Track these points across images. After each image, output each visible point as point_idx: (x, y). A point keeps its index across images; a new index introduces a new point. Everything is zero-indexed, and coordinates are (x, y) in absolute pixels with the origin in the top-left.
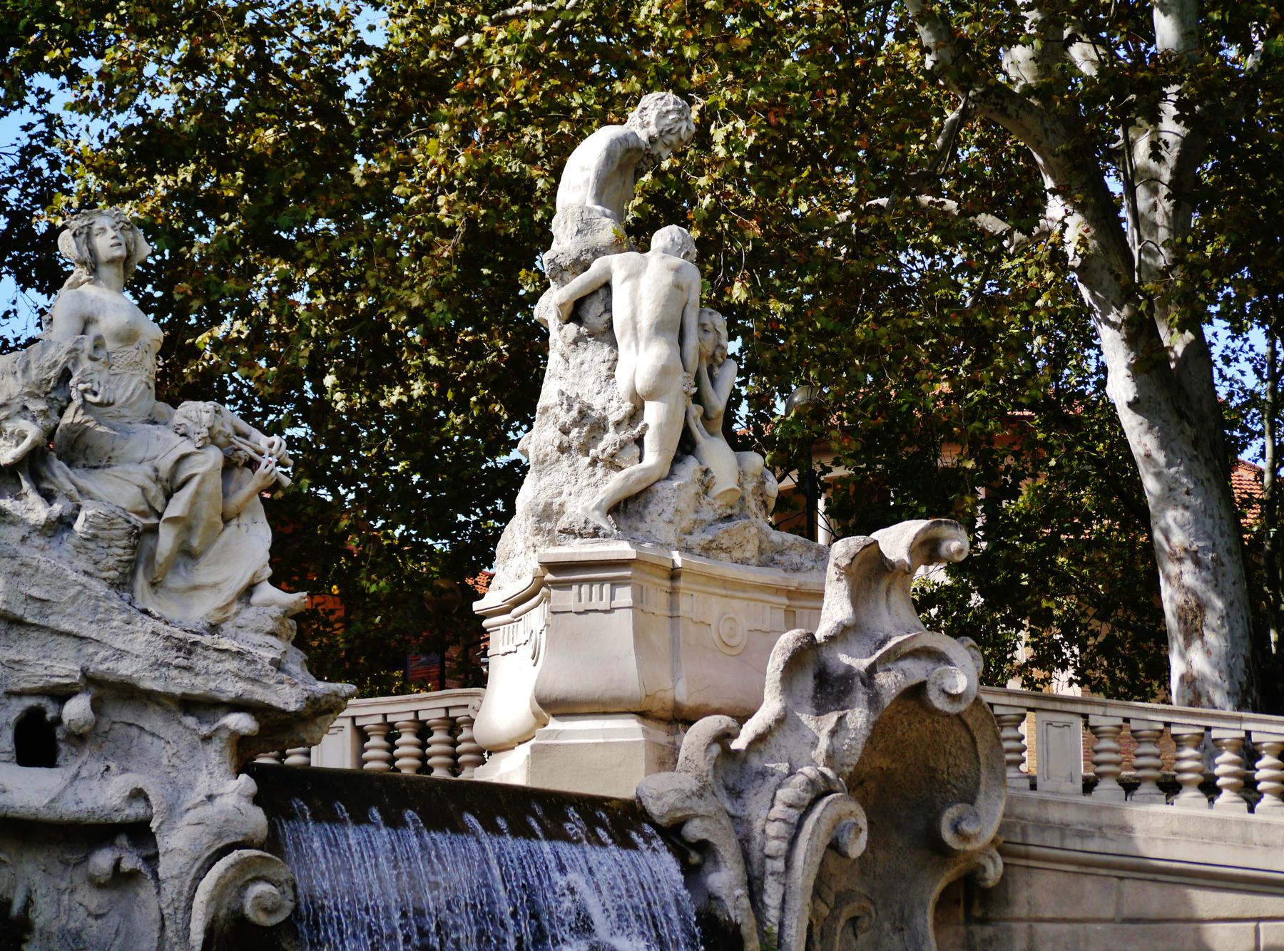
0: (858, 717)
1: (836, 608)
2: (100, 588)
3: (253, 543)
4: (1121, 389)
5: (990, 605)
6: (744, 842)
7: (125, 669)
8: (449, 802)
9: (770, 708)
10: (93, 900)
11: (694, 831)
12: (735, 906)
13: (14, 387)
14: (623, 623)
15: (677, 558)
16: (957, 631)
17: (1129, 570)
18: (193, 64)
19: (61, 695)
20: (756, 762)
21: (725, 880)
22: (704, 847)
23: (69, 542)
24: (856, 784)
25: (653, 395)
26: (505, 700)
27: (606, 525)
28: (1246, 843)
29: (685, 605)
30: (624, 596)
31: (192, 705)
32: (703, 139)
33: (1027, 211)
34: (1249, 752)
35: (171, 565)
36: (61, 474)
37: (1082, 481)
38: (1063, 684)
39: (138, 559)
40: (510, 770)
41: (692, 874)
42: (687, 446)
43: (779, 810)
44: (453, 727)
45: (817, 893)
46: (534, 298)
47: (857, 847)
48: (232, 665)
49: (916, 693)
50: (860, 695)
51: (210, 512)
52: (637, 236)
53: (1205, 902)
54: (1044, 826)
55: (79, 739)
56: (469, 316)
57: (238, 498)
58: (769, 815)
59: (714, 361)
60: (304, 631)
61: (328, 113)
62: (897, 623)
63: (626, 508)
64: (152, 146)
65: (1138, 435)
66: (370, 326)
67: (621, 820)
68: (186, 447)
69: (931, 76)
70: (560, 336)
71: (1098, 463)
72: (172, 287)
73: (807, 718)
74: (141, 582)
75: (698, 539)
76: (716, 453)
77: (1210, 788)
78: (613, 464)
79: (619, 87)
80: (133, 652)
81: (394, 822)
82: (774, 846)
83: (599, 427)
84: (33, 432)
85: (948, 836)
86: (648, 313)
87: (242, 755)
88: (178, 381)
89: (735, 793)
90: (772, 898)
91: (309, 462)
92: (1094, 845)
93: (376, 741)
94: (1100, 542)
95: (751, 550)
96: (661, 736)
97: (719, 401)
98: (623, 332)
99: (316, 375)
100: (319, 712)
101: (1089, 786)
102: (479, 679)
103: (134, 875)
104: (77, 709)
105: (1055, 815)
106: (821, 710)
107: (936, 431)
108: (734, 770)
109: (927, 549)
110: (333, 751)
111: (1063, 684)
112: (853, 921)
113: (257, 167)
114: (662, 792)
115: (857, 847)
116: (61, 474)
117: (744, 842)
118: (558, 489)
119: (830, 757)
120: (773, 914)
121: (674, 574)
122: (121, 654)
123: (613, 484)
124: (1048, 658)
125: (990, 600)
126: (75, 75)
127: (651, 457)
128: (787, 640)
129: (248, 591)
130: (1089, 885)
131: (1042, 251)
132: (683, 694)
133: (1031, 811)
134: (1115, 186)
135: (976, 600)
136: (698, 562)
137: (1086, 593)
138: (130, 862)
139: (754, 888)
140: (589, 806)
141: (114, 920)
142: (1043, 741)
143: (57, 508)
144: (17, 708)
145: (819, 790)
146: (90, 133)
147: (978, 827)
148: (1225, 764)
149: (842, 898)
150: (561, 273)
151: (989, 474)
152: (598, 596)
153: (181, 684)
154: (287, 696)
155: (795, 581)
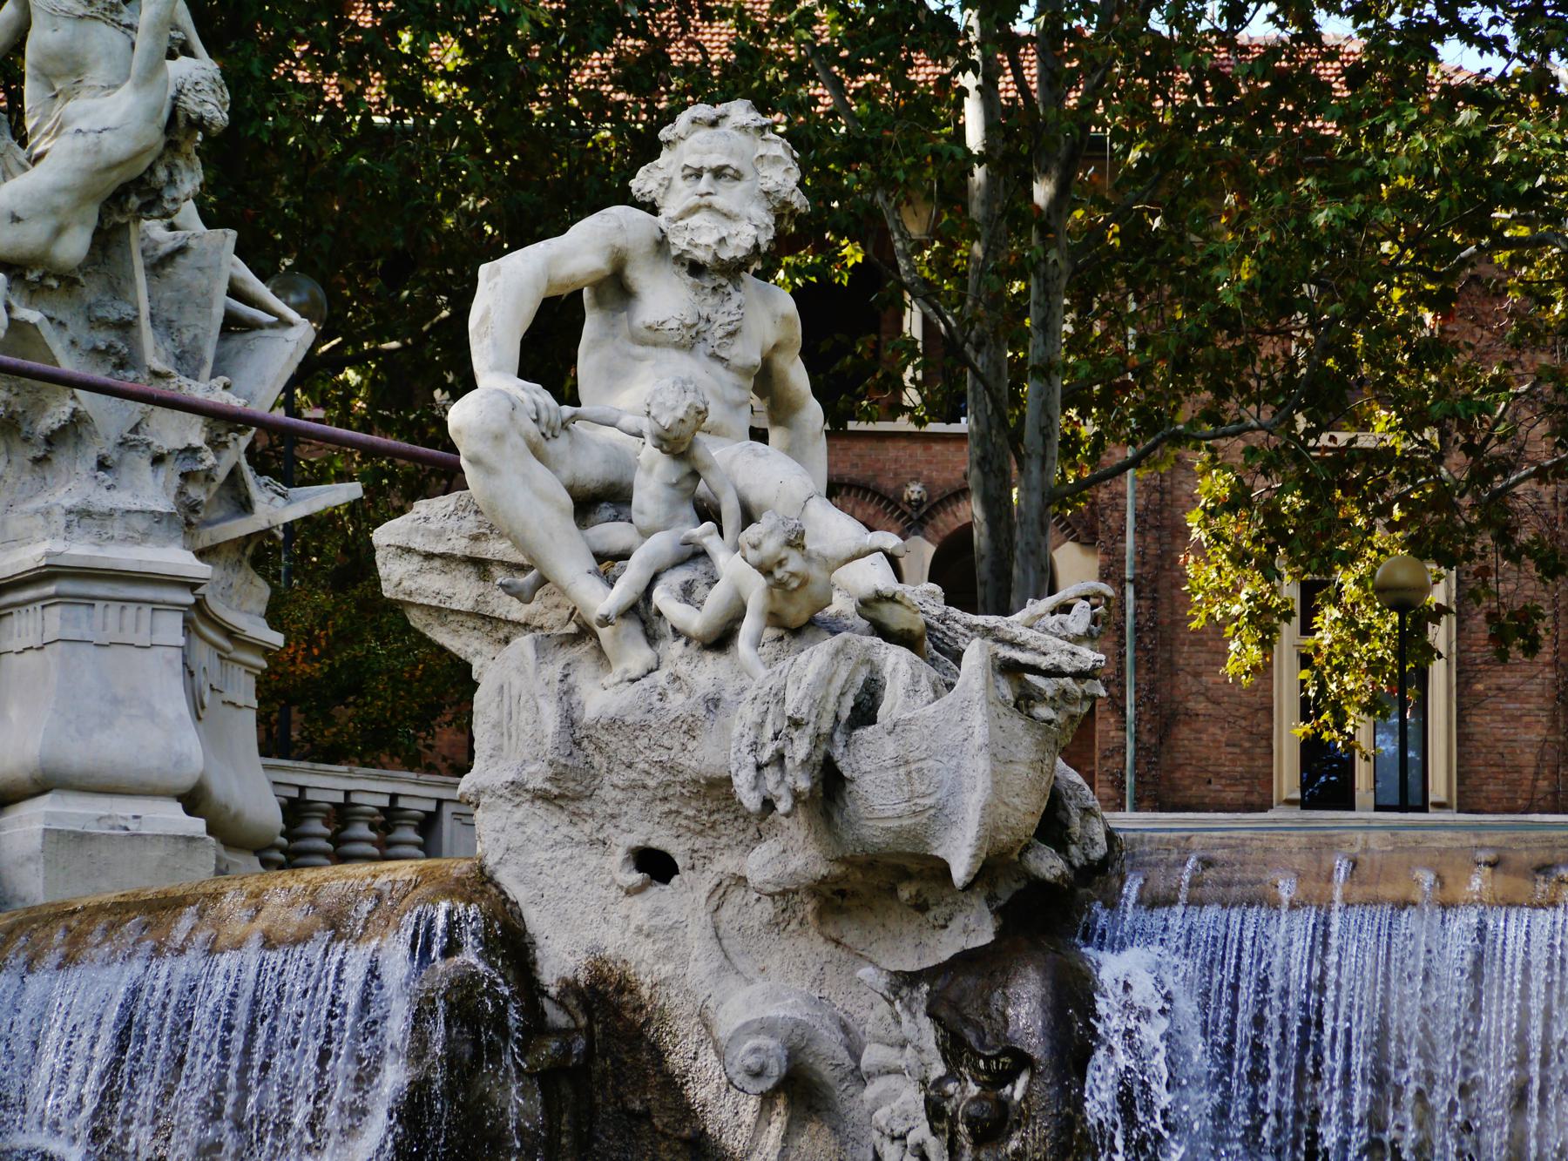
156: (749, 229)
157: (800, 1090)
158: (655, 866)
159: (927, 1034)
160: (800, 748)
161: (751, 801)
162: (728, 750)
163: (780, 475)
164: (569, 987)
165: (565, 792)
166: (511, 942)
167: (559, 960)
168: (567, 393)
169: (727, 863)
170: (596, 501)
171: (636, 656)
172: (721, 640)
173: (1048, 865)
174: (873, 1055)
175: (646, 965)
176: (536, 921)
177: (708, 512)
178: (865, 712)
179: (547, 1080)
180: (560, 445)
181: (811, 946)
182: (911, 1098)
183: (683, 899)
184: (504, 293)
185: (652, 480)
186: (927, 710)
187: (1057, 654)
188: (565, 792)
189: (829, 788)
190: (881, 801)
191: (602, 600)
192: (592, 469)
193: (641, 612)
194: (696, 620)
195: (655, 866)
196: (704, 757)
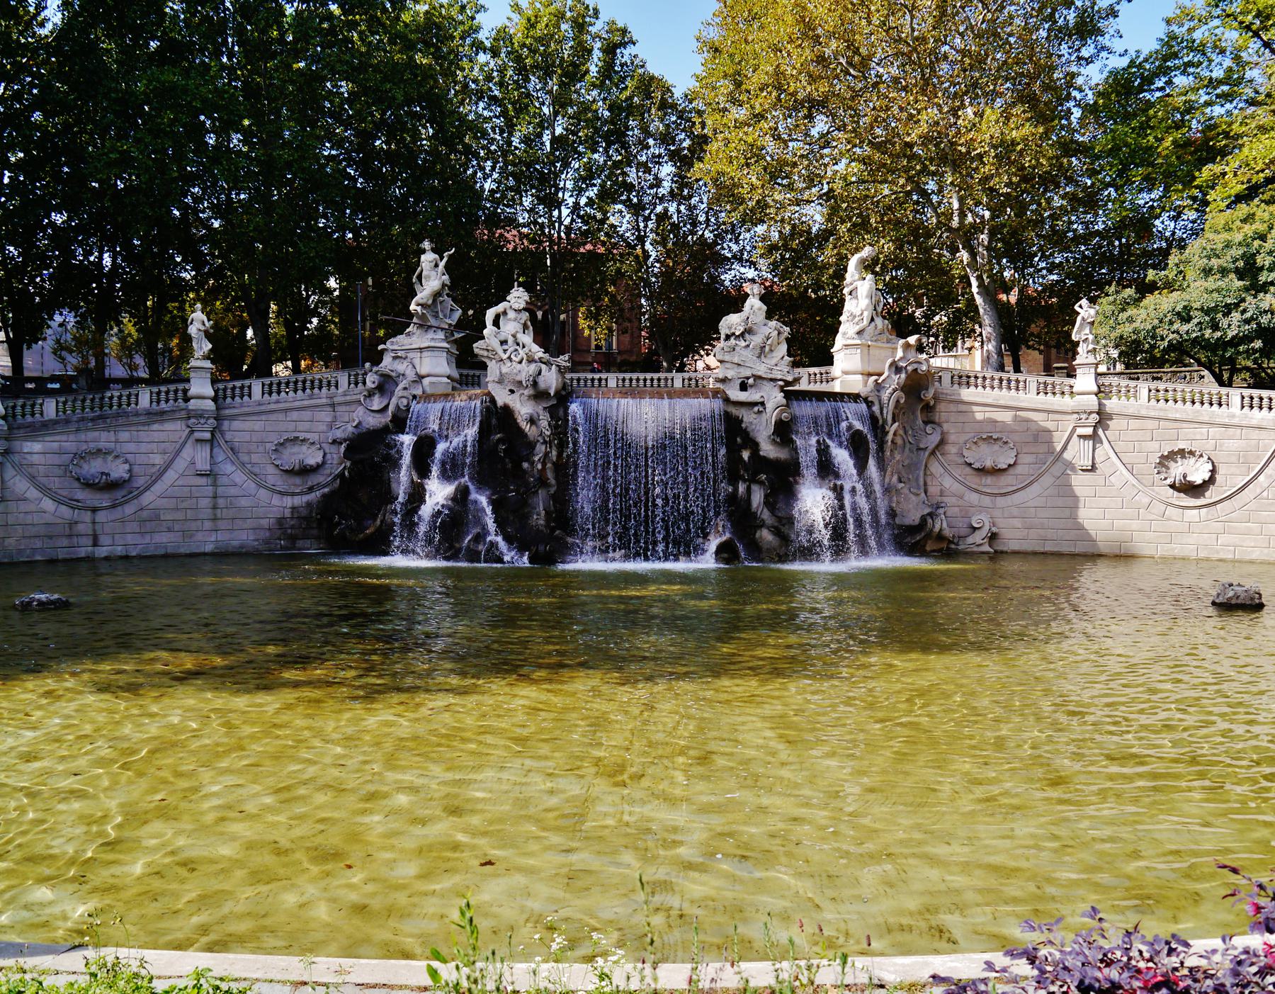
0: (903, 376)
1: (900, 354)
3: (784, 348)
19: (748, 378)
21: (876, 409)
26: (836, 370)
31: (771, 380)
34: (984, 378)
36: (747, 335)
39: (762, 352)
42: (872, 320)
47: (902, 401)
53: (975, 408)
58: (885, 396)
63: (860, 333)
67: (855, 397)
70: (848, 298)
77: (976, 386)
80: (761, 370)
81: (811, 400)
84: (742, 329)
86: (865, 293)
97: (879, 309)
98: (860, 296)
102: (832, 364)
104: (751, 381)
108: (878, 387)
115: (902, 401)
116: (747, 335)
123: (857, 328)
128: (890, 360)
140: (849, 395)
145: (895, 391)
148: (980, 381)
152: (853, 351)
153: (770, 376)
156: (523, 305)
157: (532, 421)
158: (512, 391)
162: (522, 377)
163: (527, 339)
165: (500, 382)
166: (493, 400)
167: (500, 403)
170: (504, 342)
171: (509, 364)
172: (520, 362)
175: (511, 404)
178: (540, 373)
179: (498, 419)
183: (516, 395)
184: (490, 314)
188: (500, 382)
189: (535, 384)
190: (542, 385)
191: (505, 357)
192: (502, 339)
193: (509, 358)
195: (512, 391)
196: (518, 378)
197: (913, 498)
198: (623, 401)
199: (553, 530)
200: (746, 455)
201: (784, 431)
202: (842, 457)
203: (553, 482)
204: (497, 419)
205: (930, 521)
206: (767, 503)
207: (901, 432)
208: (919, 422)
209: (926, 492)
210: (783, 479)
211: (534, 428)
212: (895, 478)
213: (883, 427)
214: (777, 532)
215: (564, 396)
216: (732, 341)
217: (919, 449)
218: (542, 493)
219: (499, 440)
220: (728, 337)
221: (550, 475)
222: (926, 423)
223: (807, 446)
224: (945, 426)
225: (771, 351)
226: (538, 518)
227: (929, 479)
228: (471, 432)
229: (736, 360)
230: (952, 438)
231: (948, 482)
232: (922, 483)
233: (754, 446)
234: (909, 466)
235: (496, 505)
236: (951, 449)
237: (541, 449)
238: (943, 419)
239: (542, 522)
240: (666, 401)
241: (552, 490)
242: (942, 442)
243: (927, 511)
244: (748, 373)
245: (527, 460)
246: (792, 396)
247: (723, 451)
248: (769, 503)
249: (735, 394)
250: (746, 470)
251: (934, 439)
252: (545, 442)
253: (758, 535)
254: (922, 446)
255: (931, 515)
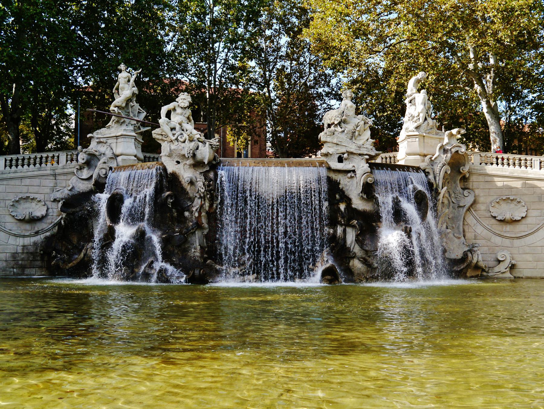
0: (449, 155)
1: (446, 140)
2: (348, 140)
3: (368, 133)
4: (485, 110)
5: (466, 140)
6: (434, 172)
7: (352, 150)
8: (394, 167)
9: (437, 154)
10: (348, 180)
11: (427, 170)
12: (432, 180)
13: (337, 114)
14: (417, 143)
15: (424, 134)
16: (462, 143)
17: (486, 135)
18: (359, 71)
19: (343, 154)
20: (435, 161)
22: (428, 172)
23: (344, 134)
24: (449, 164)
25: (421, 112)
27: (415, 130)
28: (502, 171)
29: (425, 141)
30: (417, 139)
31: (360, 155)
32: (428, 78)
33: (472, 86)
35: (357, 137)
37: (479, 123)
38: (476, 150)
39: (353, 136)
40: (401, 163)
41: (426, 176)
43: (438, 167)
44: (394, 157)
45: (443, 178)
46: (404, 100)
48: (365, 149)
49: (457, 152)
50: (449, 152)
51: (362, 129)
52: (419, 91)
53: (496, 179)
54: (474, 169)
55: (346, 159)
56: (396, 103)
57: (366, 128)
58: (437, 168)
59: (429, 108)
60: (375, 145)
61: (377, 76)
62: (455, 143)
64: (354, 82)
65: (488, 117)
66: (383, 104)
67: (417, 169)
68: (359, 121)
69: (459, 68)
71: (482, 121)
72: (357, 100)
73: (442, 155)
74: (353, 139)
75: (427, 132)
76: (429, 120)
78: (416, 122)
79: (416, 71)
80: (353, 148)
82: (438, 172)
83: (414, 117)
84: (339, 120)
85: (461, 171)
87: (367, 160)
88: (358, 112)
89: (432, 165)
90: (437, 179)
91: (375, 123)
92: (481, 172)
93: (384, 159)
94: (481, 131)
95: (434, 133)
96: (422, 158)
99: (375, 111)
100: (377, 155)
101: (481, 164)
103: (353, 177)
105: (476, 168)
106: (444, 154)
107: (459, 117)
109: (459, 132)
110: (379, 161)
111: (476, 150)
112: (448, 182)
113: (367, 84)
114: (422, 165)
115: (449, 172)
116: (342, 124)
117: (434, 172)
118: (408, 125)
119: (445, 160)
120: (437, 181)
121: (424, 137)
122: (351, 148)
124: (474, 147)
125: (467, 138)
126: (343, 73)
127: (421, 121)
128: (439, 145)
129: (368, 140)
130: (481, 177)
131: (474, 92)
132: (425, 152)
133: (473, 167)
134: (484, 83)
135: (465, 139)
136: (427, 135)
137: (480, 138)
138: (353, 175)
139: (435, 178)
140: (413, 167)
141: (351, 183)
142: (474, 158)
143: (343, 129)
144: (338, 155)
146: (345, 80)
147: (465, 170)
149: (447, 179)
150: (408, 96)
151: (466, 122)
153: (359, 152)
154: (373, 153)
155: (440, 137)
157: (192, 183)
158: (178, 162)
159: (203, 178)
160: (191, 152)
161: (187, 157)
162: (185, 152)
164: (170, 173)
165: (170, 156)
166: (165, 169)
167: (170, 170)
168: (170, 119)
169: (185, 162)
170: (173, 129)
171: (176, 143)
172: (184, 142)
173: (214, 162)
174: (198, 180)
175: (177, 172)
176: (167, 167)
177: (183, 130)
178: (197, 148)
180: (169, 124)
181: (192, 170)
182: (202, 183)
185: (178, 127)
186: (203, 148)
187: (215, 143)
188: (170, 156)
189: (194, 156)
190: (199, 156)
194: (182, 140)
195: (178, 162)
196: (183, 153)
197: (456, 240)
198: (256, 168)
199: (205, 260)
200: (342, 207)
201: (369, 190)
202: (409, 208)
203: (206, 226)
204: (168, 182)
205: (470, 255)
206: (357, 241)
207: (447, 195)
208: (459, 188)
209: (464, 236)
210: (369, 224)
211: (193, 187)
212: (444, 226)
213: (437, 189)
214: (364, 261)
215: (214, 165)
216: (332, 127)
217: (460, 207)
218: (198, 234)
219: (168, 195)
220: (329, 126)
221: (204, 221)
222: (464, 189)
223: (386, 201)
224: (477, 191)
225: (360, 135)
226: (195, 252)
227: (466, 228)
228: (149, 191)
229: (335, 141)
230: (481, 200)
231: (479, 230)
232: (461, 230)
233: (348, 201)
234: (453, 218)
235: (165, 242)
236: (481, 207)
237: (197, 202)
238: (475, 187)
239: (198, 254)
240: (286, 169)
241: (206, 232)
242: (475, 202)
243: (466, 249)
244: (343, 150)
245: (188, 210)
246: (373, 166)
247: (326, 204)
248: (359, 241)
249: (335, 165)
250: (343, 217)
251: (469, 201)
252: (201, 197)
253: (351, 264)
254: (461, 204)
255: (470, 251)
